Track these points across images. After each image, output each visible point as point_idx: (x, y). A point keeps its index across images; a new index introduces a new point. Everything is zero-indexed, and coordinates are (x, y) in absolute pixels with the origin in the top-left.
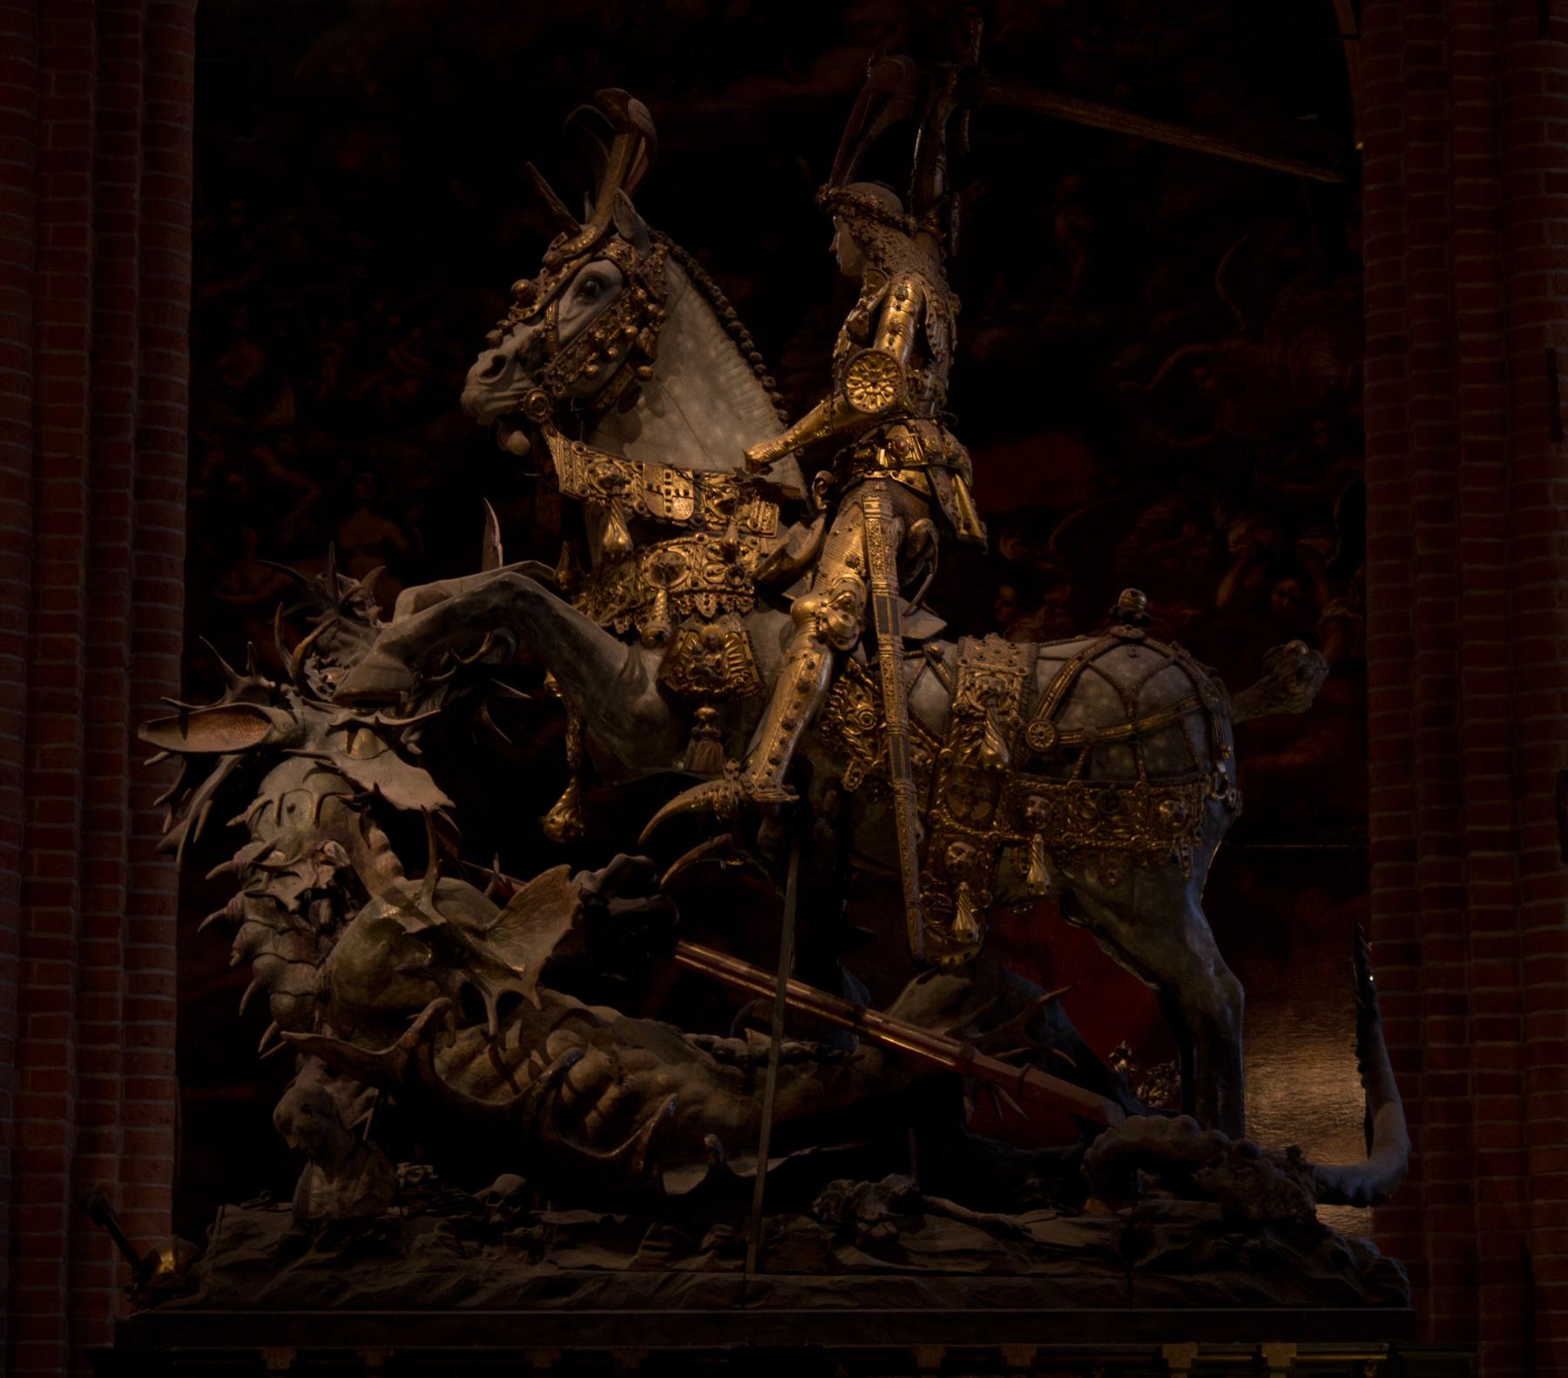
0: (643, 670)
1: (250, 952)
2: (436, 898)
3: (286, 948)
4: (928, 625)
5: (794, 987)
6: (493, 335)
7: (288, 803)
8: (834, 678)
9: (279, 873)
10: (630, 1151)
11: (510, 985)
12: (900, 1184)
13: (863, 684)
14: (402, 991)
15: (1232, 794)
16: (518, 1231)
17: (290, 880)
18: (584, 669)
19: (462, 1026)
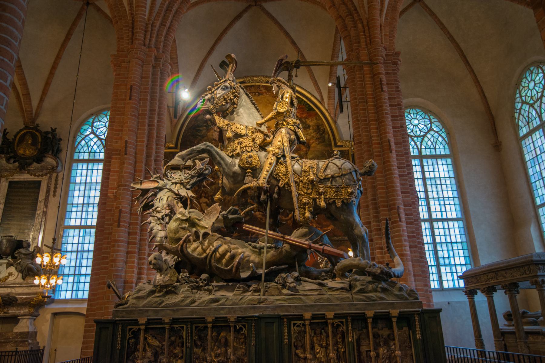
0: (235, 163)
1: (152, 230)
2: (189, 213)
3: (159, 228)
5: (269, 232)
8: (277, 164)
9: (159, 212)
10: (233, 266)
11: (205, 230)
12: (296, 274)
13: (283, 165)
15: (362, 189)
16: (206, 287)
17: (161, 213)
18: (222, 162)
19: (194, 241)
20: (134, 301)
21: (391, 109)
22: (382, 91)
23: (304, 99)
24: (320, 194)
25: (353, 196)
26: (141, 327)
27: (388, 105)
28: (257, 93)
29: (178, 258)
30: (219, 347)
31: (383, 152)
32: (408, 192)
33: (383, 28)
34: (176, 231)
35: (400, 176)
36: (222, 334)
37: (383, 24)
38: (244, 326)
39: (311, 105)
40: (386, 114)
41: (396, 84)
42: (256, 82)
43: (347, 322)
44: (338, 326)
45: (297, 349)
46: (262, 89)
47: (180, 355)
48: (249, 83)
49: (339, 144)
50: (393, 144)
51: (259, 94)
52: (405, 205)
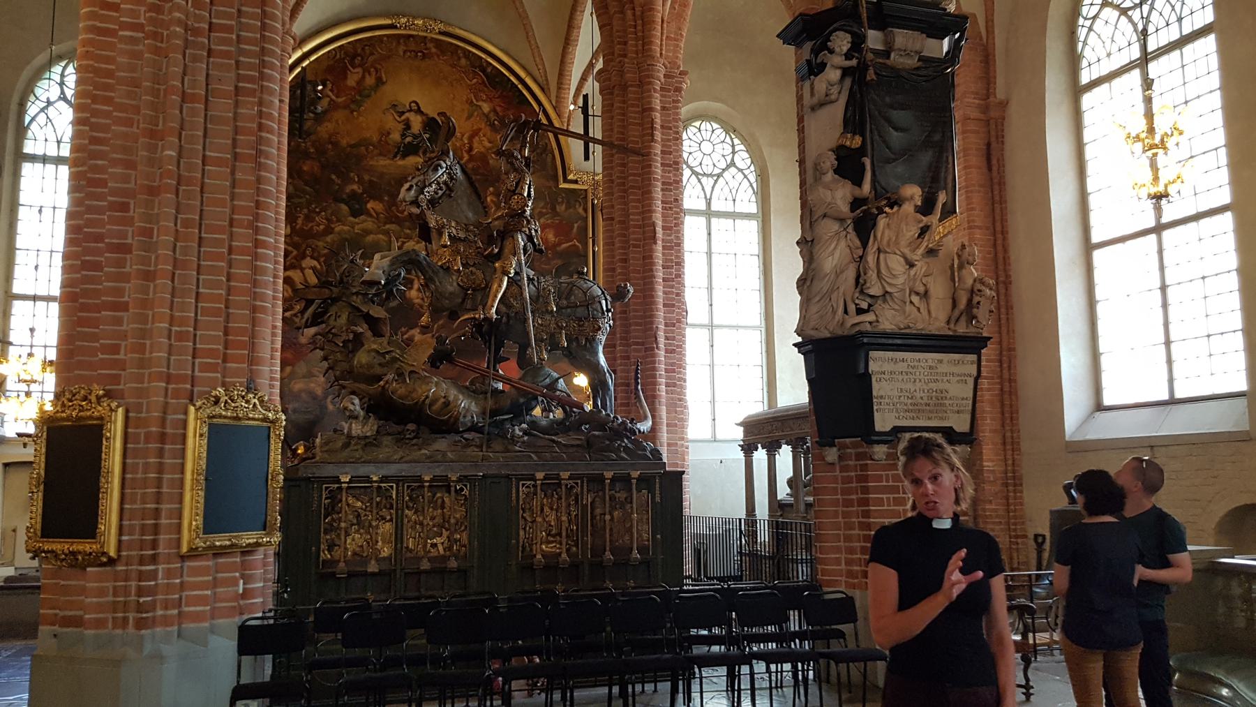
4: (532, 273)
6: (410, 178)
7: (339, 314)
9: (335, 335)
10: (450, 417)
11: (412, 369)
14: (378, 370)
15: (611, 322)
20: (326, 455)
21: (663, 171)
22: (653, 140)
23: (512, 78)
24: (561, 328)
25: (600, 332)
26: (343, 485)
27: (659, 165)
28: (419, 54)
29: (369, 400)
30: (435, 509)
31: (644, 240)
32: (673, 306)
33: (665, 25)
34: (370, 366)
35: (664, 280)
36: (439, 495)
37: (665, 19)
38: (466, 486)
39: (525, 92)
40: (657, 180)
41: (675, 127)
42: (417, 28)
43: (582, 483)
44: (572, 487)
45: (524, 512)
46: (430, 45)
47: (388, 518)
48: (405, 29)
49: (571, 177)
50: (659, 230)
51: (424, 56)
52: (666, 325)
